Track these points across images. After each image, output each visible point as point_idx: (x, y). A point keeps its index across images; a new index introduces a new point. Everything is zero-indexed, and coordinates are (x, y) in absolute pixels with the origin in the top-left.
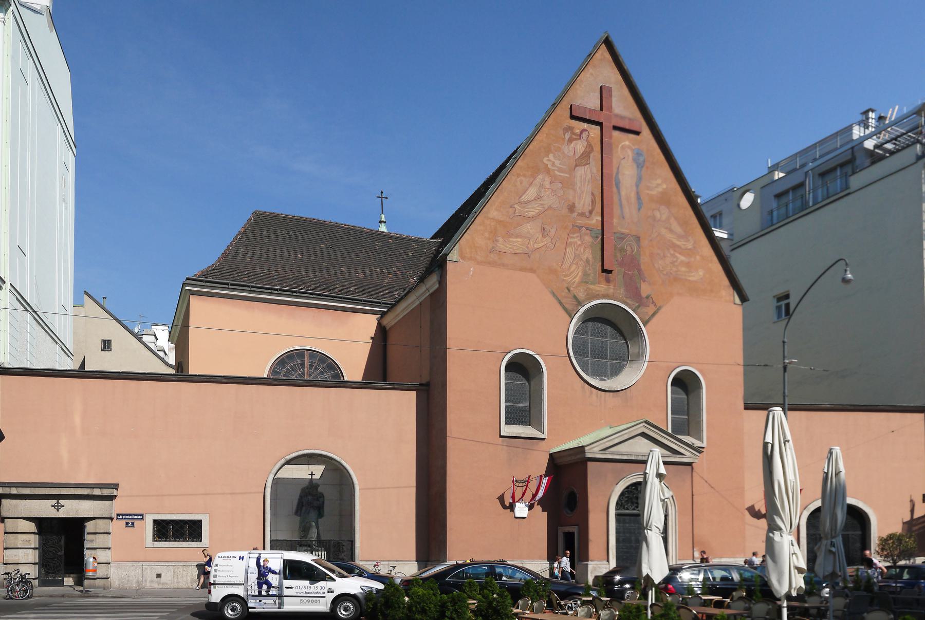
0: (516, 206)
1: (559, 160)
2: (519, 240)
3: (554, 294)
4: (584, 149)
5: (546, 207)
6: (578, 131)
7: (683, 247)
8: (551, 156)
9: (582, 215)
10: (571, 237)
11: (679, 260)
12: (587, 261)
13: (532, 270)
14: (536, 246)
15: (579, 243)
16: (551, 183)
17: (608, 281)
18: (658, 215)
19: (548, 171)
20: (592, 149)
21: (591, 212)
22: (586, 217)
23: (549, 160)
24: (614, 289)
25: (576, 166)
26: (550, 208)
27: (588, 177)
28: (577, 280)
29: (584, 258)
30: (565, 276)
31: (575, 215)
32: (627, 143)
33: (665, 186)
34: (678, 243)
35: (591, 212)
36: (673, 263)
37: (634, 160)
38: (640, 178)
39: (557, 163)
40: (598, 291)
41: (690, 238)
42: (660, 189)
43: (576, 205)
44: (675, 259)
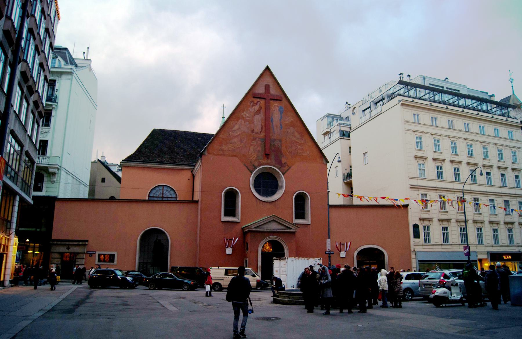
0: (230, 132)
1: (248, 113)
2: (231, 145)
3: (245, 165)
4: (258, 108)
5: (242, 131)
6: (256, 102)
7: (300, 142)
8: (245, 113)
9: (257, 133)
10: (252, 142)
11: (298, 148)
12: (259, 151)
13: (236, 156)
14: (238, 147)
15: (256, 144)
16: (245, 122)
17: (268, 158)
18: (289, 131)
19: (243, 118)
20: (262, 108)
21: (261, 132)
22: (258, 134)
23: (244, 114)
24: (270, 161)
25: (255, 115)
26: (244, 132)
27: (260, 118)
28: (254, 158)
29: (258, 150)
30: (250, 157)
31: (254, 134)
32: (276, 104)
33: (292, 119)
34: (298, 141)
35: (261, 132)
36: (296, 149)
37: (279, 110)
38: (281, 117)
39: (247, 115)
40: (263, 162)
41: (303, 139)
42: (290, 121)
43: (255, 129)
44: (296, 148)
